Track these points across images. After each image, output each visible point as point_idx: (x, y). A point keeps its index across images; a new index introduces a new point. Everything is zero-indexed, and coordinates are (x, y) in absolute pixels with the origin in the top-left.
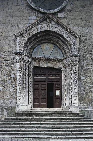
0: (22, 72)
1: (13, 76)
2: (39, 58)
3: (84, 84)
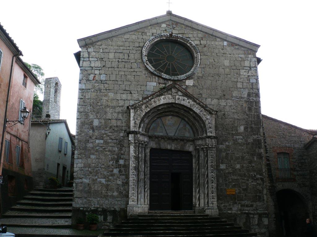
0: (137, 158)
1: (121, 162)
2: (159, 137)
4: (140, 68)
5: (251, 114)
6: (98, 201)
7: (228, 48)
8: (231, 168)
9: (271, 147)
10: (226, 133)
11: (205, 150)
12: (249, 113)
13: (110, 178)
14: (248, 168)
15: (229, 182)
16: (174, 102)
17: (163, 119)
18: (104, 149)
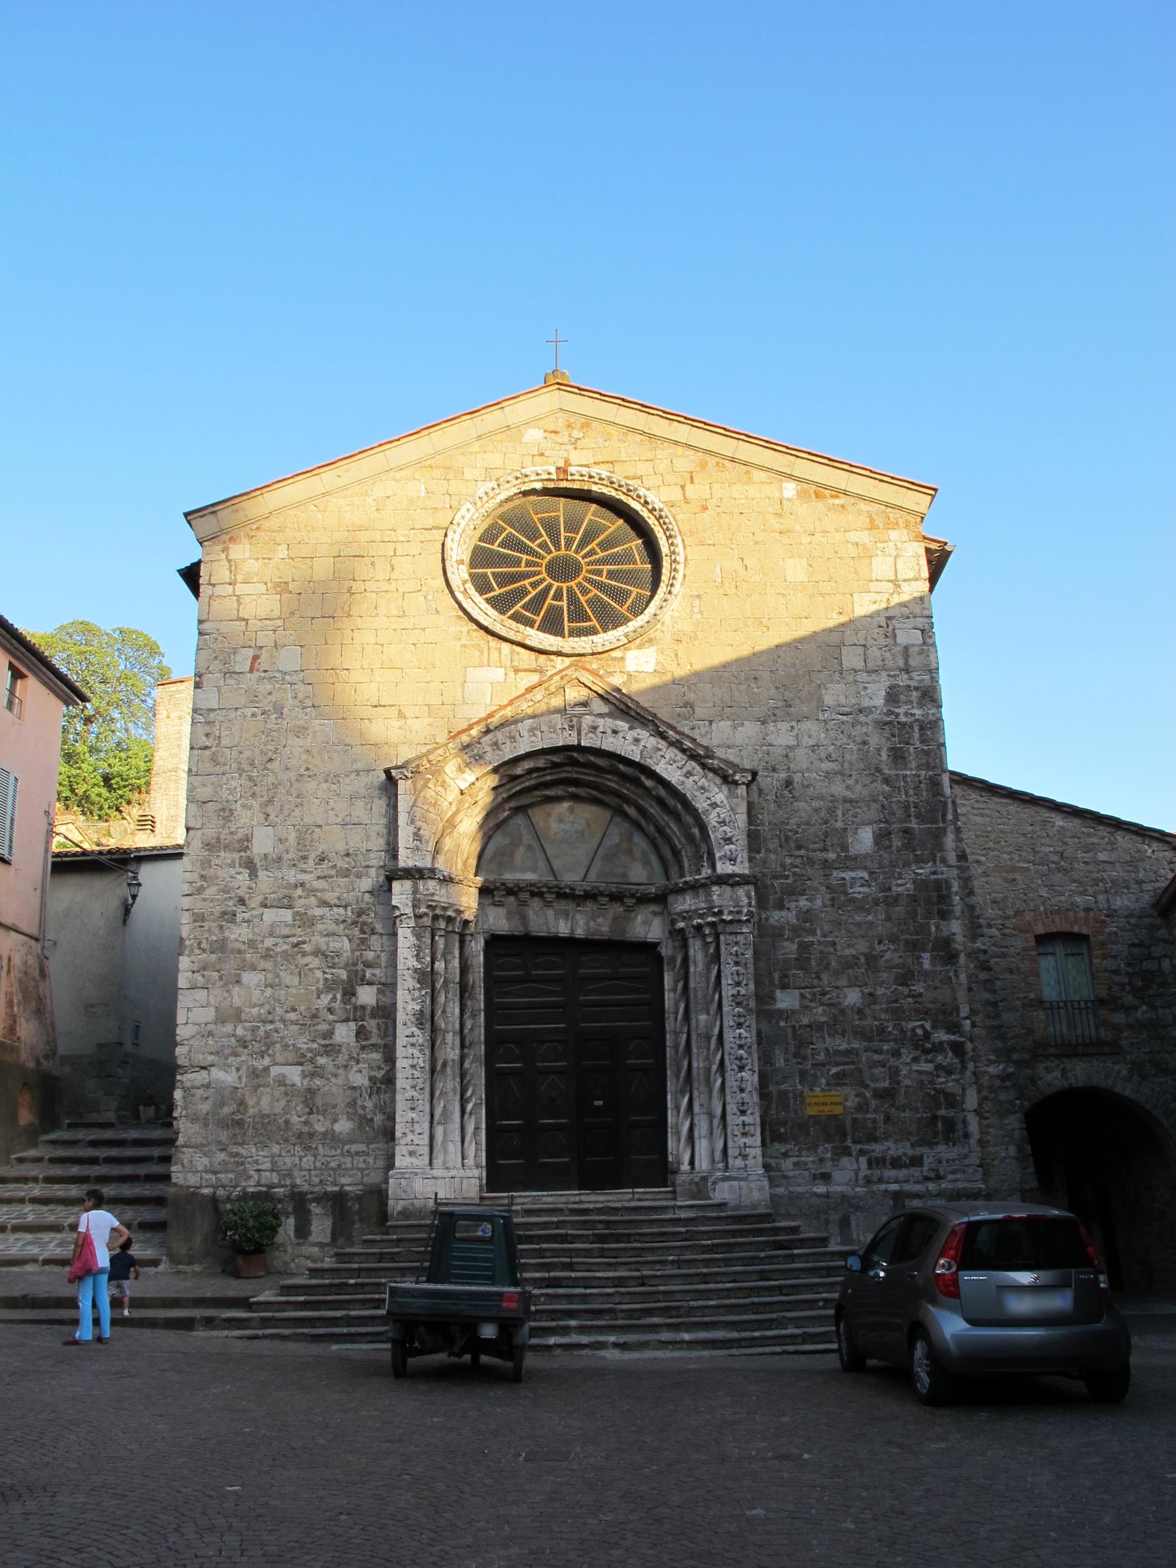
0: (427, 978)
1: (367, 996)
2: (521, 889)
3: (795, 1036)
4: (437, 612)
5: (905, 776)
6: (273, 1156)
7: (802, 509)
8: (823, 1004)
9: (1010, 912)
10: (798, 861)
11: (707, 932)
12: (893, 772)
13: (321, 1061)
14: (896, 1001)
15: (813, 1065)
16: (576, 743)
17: (537, 814)
18: (296, 945)
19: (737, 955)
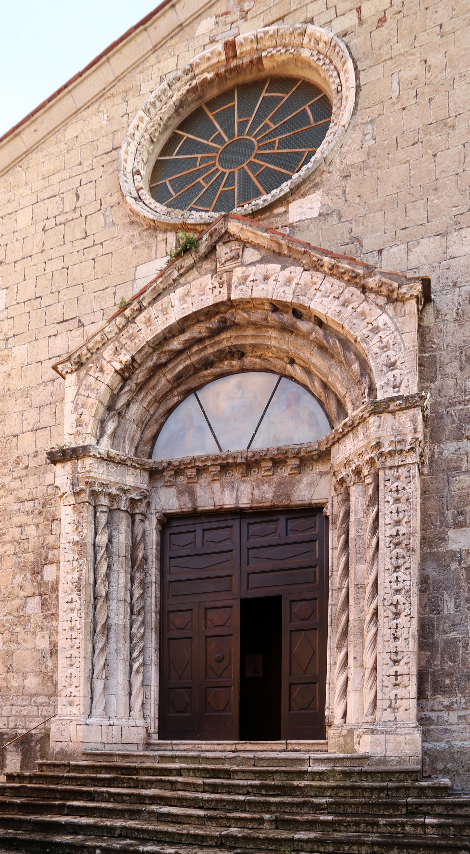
19: (397, 491)
